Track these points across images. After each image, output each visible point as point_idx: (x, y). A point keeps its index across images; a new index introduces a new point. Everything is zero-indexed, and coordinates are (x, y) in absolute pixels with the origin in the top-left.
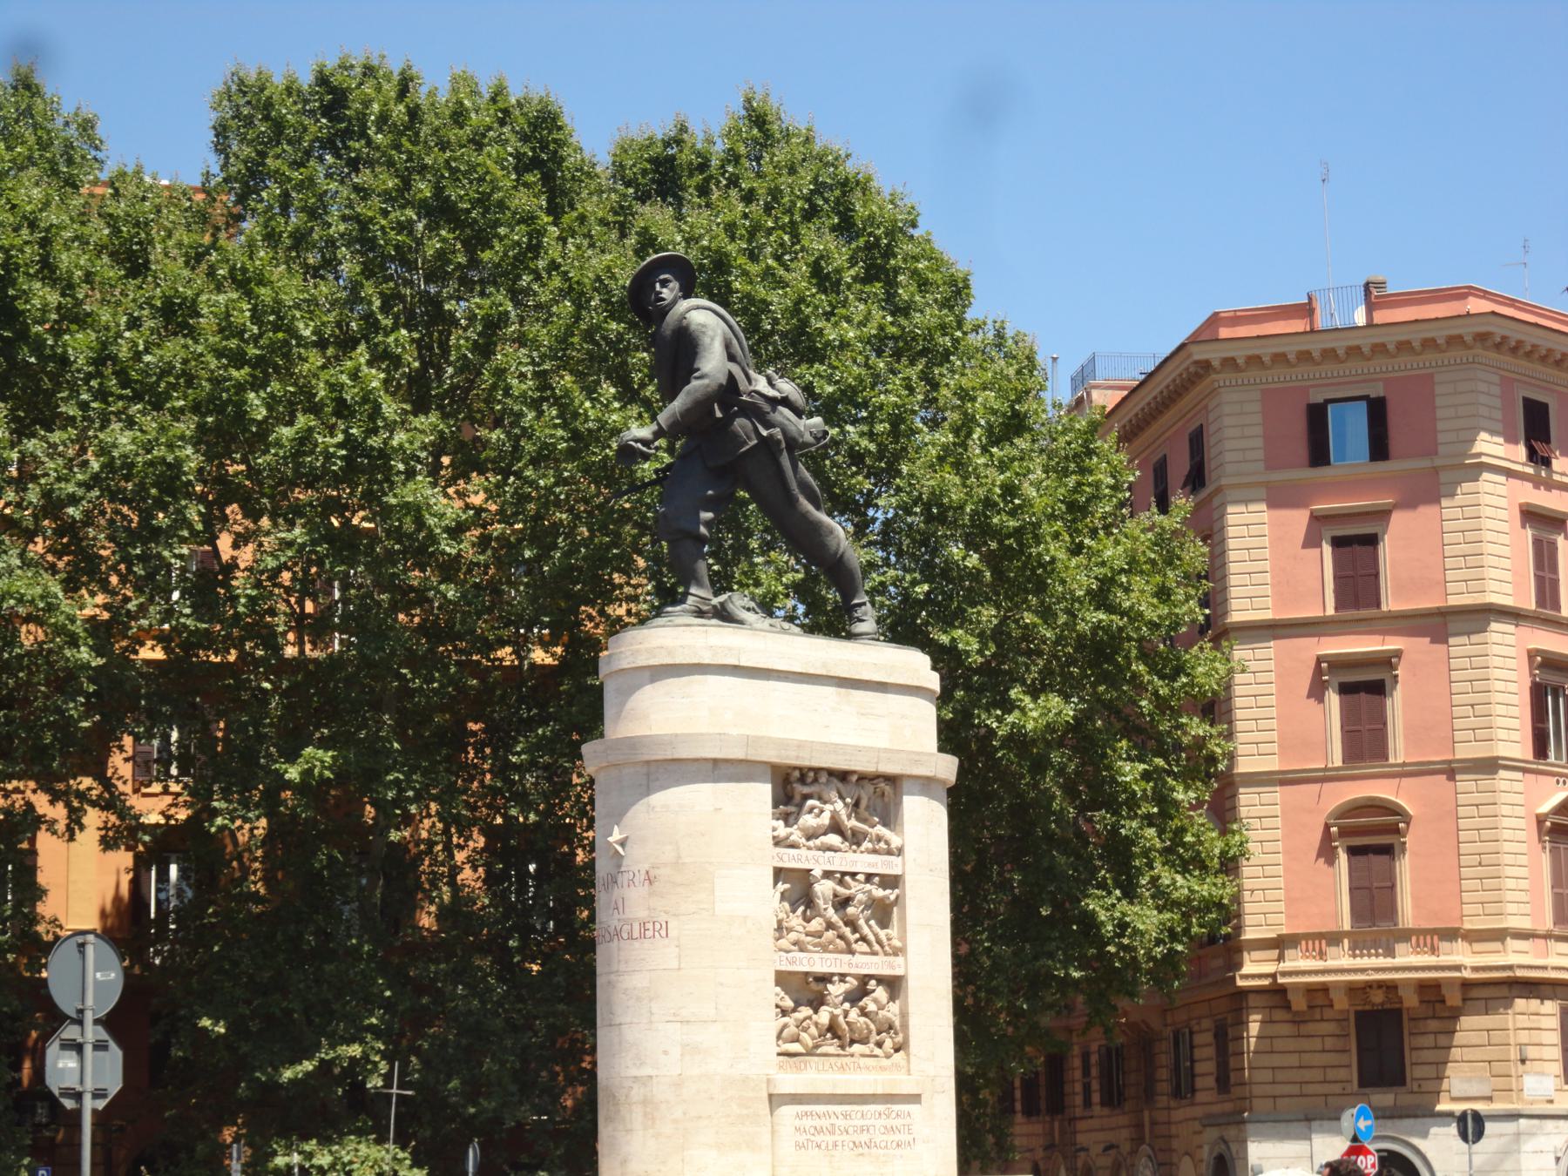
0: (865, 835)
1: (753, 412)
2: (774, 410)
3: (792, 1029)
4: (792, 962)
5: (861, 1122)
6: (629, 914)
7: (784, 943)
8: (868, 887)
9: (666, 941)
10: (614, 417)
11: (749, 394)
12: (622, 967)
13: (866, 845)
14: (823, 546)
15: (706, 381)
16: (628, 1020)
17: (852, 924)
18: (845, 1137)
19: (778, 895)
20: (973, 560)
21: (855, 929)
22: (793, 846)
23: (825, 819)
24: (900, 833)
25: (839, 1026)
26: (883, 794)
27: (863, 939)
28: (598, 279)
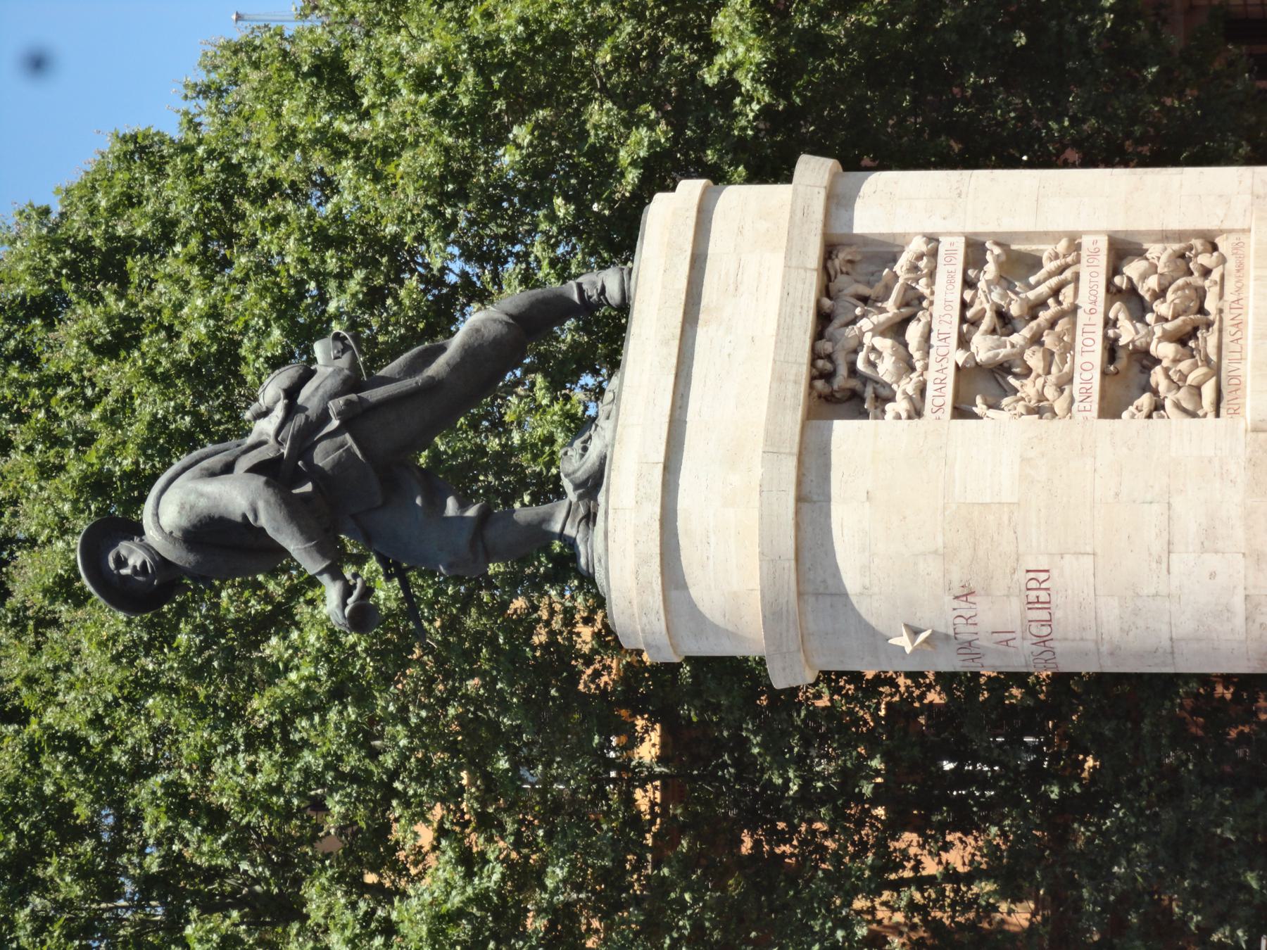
0: (908, 288)
1: (305, 439)
2: (303, 409)
3: (1183, 395)
6: (1016, 626)
7: (1060, 406)
8: (982, 285)
9: (1055, 573)
10: (312, 638)
11: (280, 444)
12: (1090, 635)
13: (922, 286)
14: (497, 342)
15: (261, 506)
16: (1165, 628)
17: (1034, 309)
19: (992, 413)
20: (521, 133)
21: (1043, 304)
22: (922, 390)
23: (885, 344)
24: (907, 237)
25: (1178, 329)
26: (850, 262)
27: (1056, 293)
28: (116, 659)
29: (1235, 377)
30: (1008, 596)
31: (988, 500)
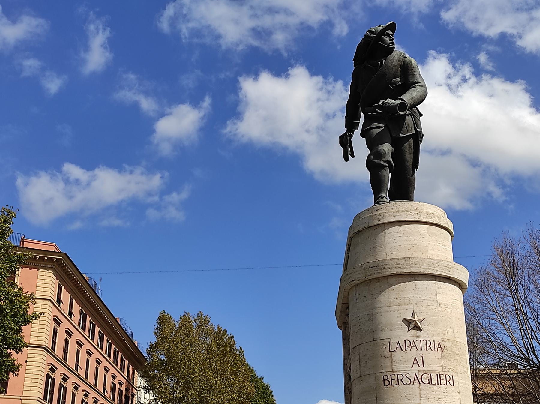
9: (453, 388)
30: (442, 366)
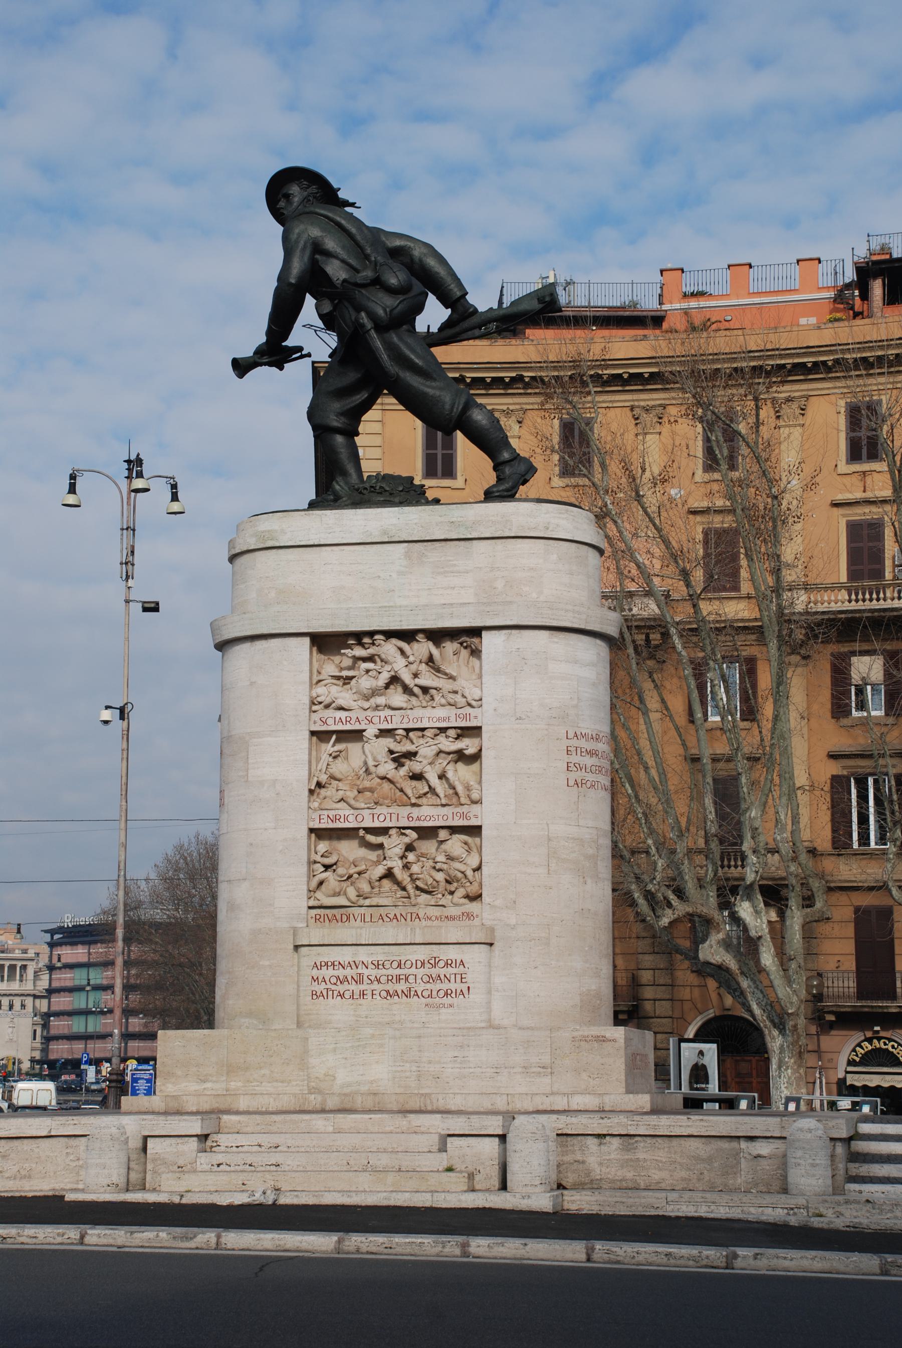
4: (336, 819)
5: (398, 971)
18: (375, 986)
22: (341, 708)
29: (348, 918)
31: (250, 761)
